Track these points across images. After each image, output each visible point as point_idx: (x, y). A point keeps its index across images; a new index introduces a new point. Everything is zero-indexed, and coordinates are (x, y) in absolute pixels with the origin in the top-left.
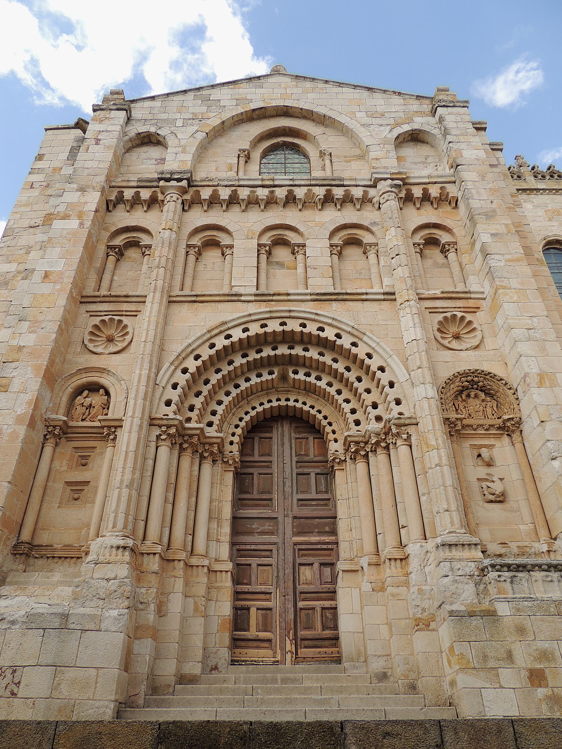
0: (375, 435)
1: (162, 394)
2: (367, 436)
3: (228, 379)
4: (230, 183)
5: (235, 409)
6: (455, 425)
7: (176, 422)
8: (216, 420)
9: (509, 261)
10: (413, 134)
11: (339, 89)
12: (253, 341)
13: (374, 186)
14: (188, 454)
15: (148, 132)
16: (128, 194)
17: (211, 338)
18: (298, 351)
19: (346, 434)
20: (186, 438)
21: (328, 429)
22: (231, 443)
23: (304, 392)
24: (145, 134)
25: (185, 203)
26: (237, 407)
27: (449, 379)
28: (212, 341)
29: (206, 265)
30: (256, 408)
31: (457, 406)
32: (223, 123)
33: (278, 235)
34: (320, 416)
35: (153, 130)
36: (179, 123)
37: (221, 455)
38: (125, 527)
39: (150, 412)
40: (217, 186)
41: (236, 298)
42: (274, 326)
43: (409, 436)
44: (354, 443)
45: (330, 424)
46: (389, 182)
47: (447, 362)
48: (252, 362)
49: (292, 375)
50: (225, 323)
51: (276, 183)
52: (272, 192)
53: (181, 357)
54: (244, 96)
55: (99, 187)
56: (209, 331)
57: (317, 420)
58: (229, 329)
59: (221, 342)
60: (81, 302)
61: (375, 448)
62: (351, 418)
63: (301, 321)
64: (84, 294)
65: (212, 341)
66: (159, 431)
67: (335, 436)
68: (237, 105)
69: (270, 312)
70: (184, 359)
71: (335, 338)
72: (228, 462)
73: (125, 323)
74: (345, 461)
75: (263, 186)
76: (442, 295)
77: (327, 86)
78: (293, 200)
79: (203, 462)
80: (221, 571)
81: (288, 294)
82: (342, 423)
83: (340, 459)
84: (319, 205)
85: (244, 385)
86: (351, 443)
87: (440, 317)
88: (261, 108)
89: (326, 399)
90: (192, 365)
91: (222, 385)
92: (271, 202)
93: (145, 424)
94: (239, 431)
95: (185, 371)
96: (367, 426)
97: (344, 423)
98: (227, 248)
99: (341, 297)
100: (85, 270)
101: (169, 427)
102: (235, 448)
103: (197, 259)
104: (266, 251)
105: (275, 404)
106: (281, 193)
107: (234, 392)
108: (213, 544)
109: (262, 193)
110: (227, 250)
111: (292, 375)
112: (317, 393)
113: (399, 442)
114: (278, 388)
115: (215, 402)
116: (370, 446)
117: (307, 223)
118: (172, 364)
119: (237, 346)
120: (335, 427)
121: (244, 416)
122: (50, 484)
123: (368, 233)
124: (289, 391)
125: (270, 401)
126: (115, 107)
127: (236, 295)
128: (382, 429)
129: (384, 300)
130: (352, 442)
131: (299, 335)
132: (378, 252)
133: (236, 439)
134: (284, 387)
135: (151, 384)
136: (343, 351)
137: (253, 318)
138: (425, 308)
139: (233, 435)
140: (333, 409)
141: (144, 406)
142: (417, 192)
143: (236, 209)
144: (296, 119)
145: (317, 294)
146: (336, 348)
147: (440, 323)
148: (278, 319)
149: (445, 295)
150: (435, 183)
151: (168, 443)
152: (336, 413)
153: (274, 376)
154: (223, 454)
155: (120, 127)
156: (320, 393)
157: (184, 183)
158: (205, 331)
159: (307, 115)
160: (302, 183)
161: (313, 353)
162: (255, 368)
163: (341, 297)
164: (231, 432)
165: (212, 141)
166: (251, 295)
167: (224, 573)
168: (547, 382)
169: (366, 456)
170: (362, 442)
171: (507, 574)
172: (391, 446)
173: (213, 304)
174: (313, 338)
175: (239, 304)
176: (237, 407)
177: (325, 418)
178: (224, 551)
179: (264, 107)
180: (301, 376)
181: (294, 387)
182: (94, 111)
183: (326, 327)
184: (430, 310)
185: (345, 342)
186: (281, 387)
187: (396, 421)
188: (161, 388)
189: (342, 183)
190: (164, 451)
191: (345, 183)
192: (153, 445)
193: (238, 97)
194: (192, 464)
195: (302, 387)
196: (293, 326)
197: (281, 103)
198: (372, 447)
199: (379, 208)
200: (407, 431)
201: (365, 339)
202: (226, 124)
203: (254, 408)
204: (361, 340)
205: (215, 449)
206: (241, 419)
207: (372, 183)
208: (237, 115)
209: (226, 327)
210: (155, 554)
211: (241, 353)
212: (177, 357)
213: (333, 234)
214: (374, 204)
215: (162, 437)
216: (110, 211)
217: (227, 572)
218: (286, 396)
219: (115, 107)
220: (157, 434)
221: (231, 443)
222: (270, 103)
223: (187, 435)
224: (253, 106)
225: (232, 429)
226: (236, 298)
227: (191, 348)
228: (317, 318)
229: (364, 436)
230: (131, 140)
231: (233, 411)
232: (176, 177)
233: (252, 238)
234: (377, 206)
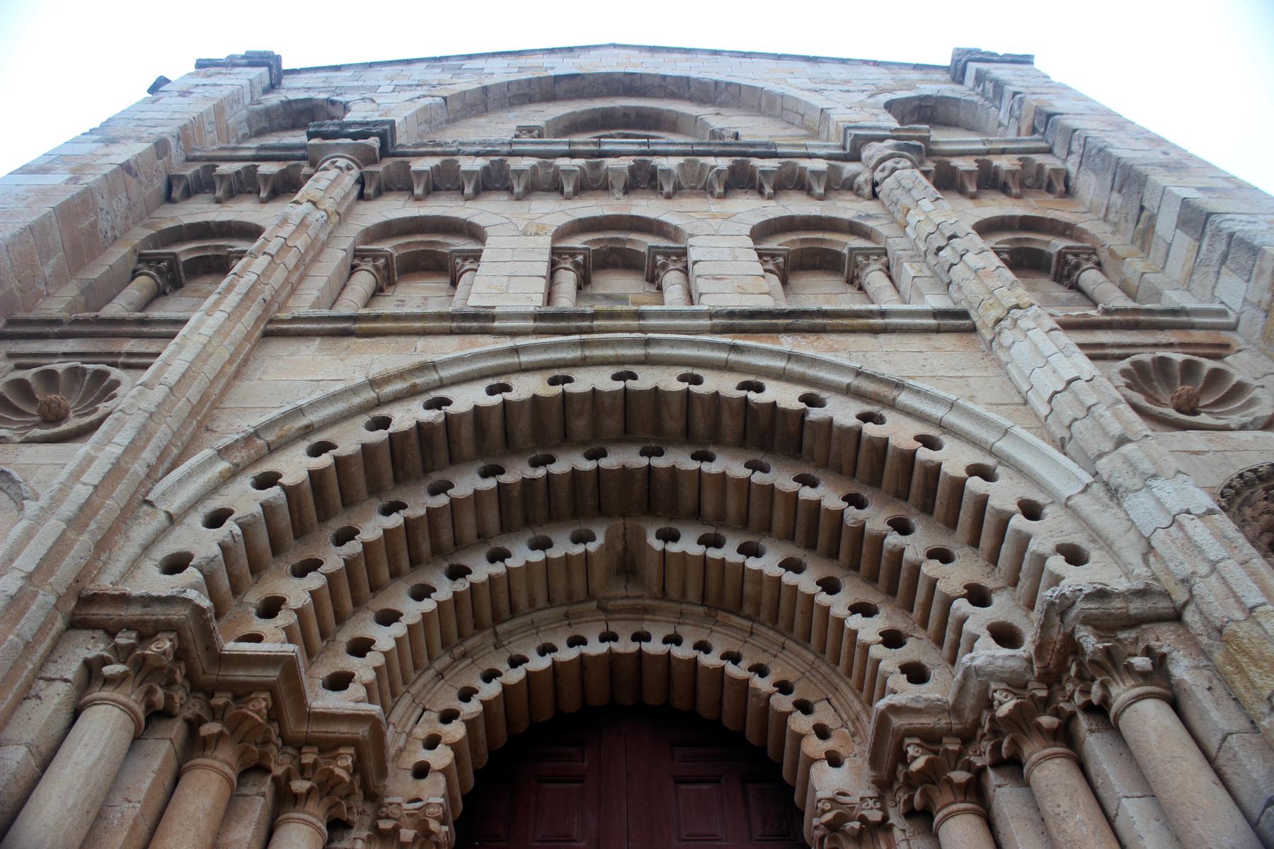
0: (1004, 686)
2: (970, 702)
3: (425, 547)
7: (178, 614)
8: (364, 669)
10: (920, 107)
12: (523, 425)
13: (855, 157)
14: (217, 764)
17: (380, 403)
19: (881, 704)
20: (219, 700)
21: (800, 723)
23: (701, 610)
24: (300, 106)
25: (367, 182)
26: (457, 651)
29: (402, 301)
30: (525, 660)
33: (611, 240)
34: (763, 685)
37: (369, 808)
43: (1160, 661)
44: (917, 741)
45: (805, 707)
46: (891, 142)
47: (1197, 453)
48: (516, 493)
49: (658, 545)
52: (598, 166)
56: (373, 383)
57: (752, 701)
58: (442, 385)
61: (1014, 742)
62: (890, 660)
65: (384, 412)
66: (102, 646)
67: (830, 744)
68: (518, 72)
70: (273, 449)
71: (803, 405)
73: (112, 377)
74: (884, 826)
78: (650, 182)
79: (286, 816)
81: (640, 315)
82: (851, 697)
83: (863, 819)
84: (716, 186)
85: (482, 570)
86: (907, 741)
89: (782, 624)
91: (405, 564)
93: (45, 598)
94: (456, 731)
95: (266, 481)
96: (968, 656)
97: (858, 697)
98: (465, 259)
100: (47, 271)
101: (146, 632)
102: (434, 792)
104: (577, 265)
105: (595, 648)
107: (445, 590)
110: (466, 263)
112: (748, 609)
113: (1121, 692)
114: (609, 599)
115: (370, 616)
116: (986, 746)
118: (222, 453)
119: (466, 432)
120: (823, 714)
121: (478, 683)
123: (854, 237)
124: (646, 610)
125: (576, 641)
127: (475, 317)
128: (1029, 660)
129: (938, 330)
130: (911, 733)
131: (676, 408)
132: (888, 268)
133: (441, 757)
134: (627, 597)
135: (122, 491)
136: (834, 442)
139: (432, 743)
140: (811, 657)
145: (731, 314)
146: (807, 441)
151: (131, 696)
152: (824, 669)
153: (592, 547)
154: (381, 806)
155: (246, 83)
156: (758, 605)
157: (374, 142)
158: (360, 378)
159: (676, 91)
161: (730, 465)
164: (422, 731)
166: (523, 316)
169: (976, 792)
170: (949, 732)
172: (1083, 723)
173: (402, 340)
174: (726, 418)
176: (457, 651)
177: (784, 688)
179: (579, 75)
180: (688, 544)
181: (663, 594)
186: (617, 598)
187: (1092, 606)
188: (162, 517)
191: (780, 150)
194: (229, 812)
195: (693, 594)
198: (996, 748)
199: (875, 196)
200: (1141, 646)
201: (904, 398)
203: (516, 662)
204: (892, 405)
205: (342, 766)
206: (466, 695)
207: (848, 151)
208: (518, 82)
209: (433, 377)
211: (481, 464)
212: (248, 439)
214: (858, 190)
218: (636, 627)
220: (91, 654)
221: (421, 771)
225: (430, 725)
227: (303, 422)
228: (734, 357)
229: (955, 710)
231: (438, 665)
233: (537, 234)
234: (867, 190)
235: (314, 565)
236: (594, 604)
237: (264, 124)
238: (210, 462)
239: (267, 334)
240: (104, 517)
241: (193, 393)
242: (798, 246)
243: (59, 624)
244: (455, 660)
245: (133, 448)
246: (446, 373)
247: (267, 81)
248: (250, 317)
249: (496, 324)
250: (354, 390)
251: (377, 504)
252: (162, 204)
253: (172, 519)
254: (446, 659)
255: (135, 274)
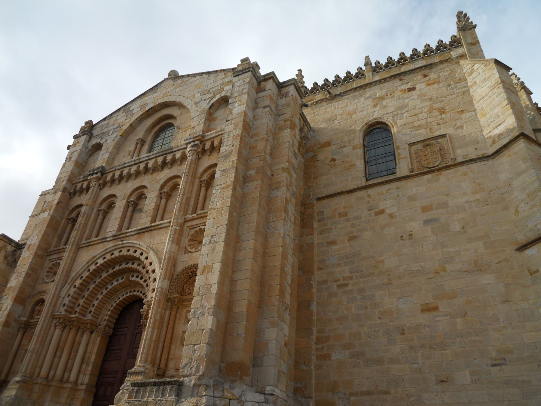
1: (62, 302)
4: (121, 167)
5: (109, 301)
6: (175, 301)
7: (61, 316)
9: (223, 188)
11: (193, 79)
15: (97, 143)
16: (79, 186)
18: (130, 265)
22: (105, 320)
26: (111, 299)
27: (180, 273)
28: (89, 268)
31: (185, 288)
32: (131, 125)
35: (98, 142)
36: (111, 133)
38: (25, 372)
39: (53, 312)
40: (116, 170)
41: (104, 240)
42: (117, 254)
46: (192, 143)
47: (185, 261)
50: (94, 257)
51: (141, 160)
53: (73, 280)
54: (145, 102)
55: (61, 190)
56: (87, 263)
58: (97, 259)
59: (93, 267)
60: (48, 256)
63: (128, 248)
64: (49, 251)
65: (89, 268)
69: (115, 246)
70: (76, 280)
72: (98, 331)
75: (135, 164)
76: (196, 217)
77: (189, 78)
80: (81, 390)
85: (110, 287)
87: (192, 232)
88: (151, 108)
90: (78, 282)
92: (138, 173)
93: (48, 318)
99: (149, 229)
101: (60, 319)
103: (105, 216)
104: (132, 205)
106: (142, 166)
107: (105, 292)
108: (81, 376)
109: (134, 169)
111: (131, 278)
117: (152, 182)
118: (68, 284)
122: (19, 351)
124: (135, 286)
126: (81, 134)
137: (108, 251)
138: (188, 227)
141: (48, 310)
142: (208, 145)
143: (123, 182)
144: (171, 107)
145: (139, 230)
147: (193, 235)
148: (117, 250)
149: (198, 216)
150: (219, 135)
157: (99, 175)
158: (85, 263)
160: (153, 156)
162: (116, 277)
163: (149, 229)
164: (106, 314)
165: (127, 137)
167: (82, 391)
168: (206, 272)
171: (136, 388)
175: (106, 243)
178: (85, 379)
180: (134, 279)
182: (74, 138)
183: (138, 250)
184: (190, 228)
185: (142, 258)
189: (171, 151)
190: (58, 332)
191: (174, 150)
192: (52, 329)
193: (142, 104)
196: (124, 252)
197: (161, 101)
202: (133, 125)
208: (139, 117)
209: (95, 259)
210: (38, 383)
211: (106, 271)
212: (72, 280)
213: (162, 187)
215: (57, 324)
216: (72, 198)
217: (83, 390)
219: (81, 134)
222: (156, 103)
223: (72, 321)
224: (147, 108)
226: (104, 240)
227: (78, 274)
230: (90, 150)
231: (108, 302)
232: (95, 172)
235: (83, 297)
236: (128, 287)
237: (91, 152)
238: (67, 286)
239: (79, 248)
240: (53, 303)
241: (64, 274)
242: (173, 184)
243: (51, 319)
244: (111, 301)
245: (56, 289)
246: (97, 257)
247: (88, 137)
248: (74, 247)
249: (107, 240)
250: (85, 265)
251: (93, 282)
252: (71, 199)
253: (64, 298)
254: (109, 301)
255: (68, 224)
